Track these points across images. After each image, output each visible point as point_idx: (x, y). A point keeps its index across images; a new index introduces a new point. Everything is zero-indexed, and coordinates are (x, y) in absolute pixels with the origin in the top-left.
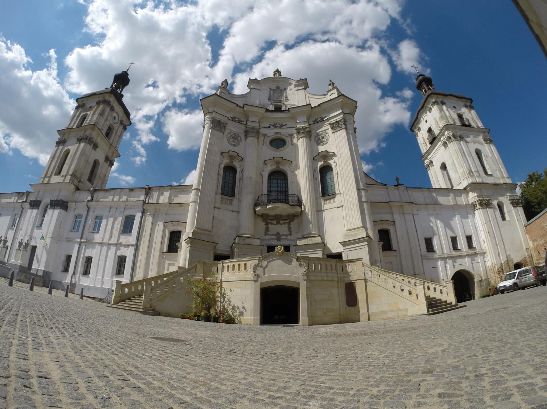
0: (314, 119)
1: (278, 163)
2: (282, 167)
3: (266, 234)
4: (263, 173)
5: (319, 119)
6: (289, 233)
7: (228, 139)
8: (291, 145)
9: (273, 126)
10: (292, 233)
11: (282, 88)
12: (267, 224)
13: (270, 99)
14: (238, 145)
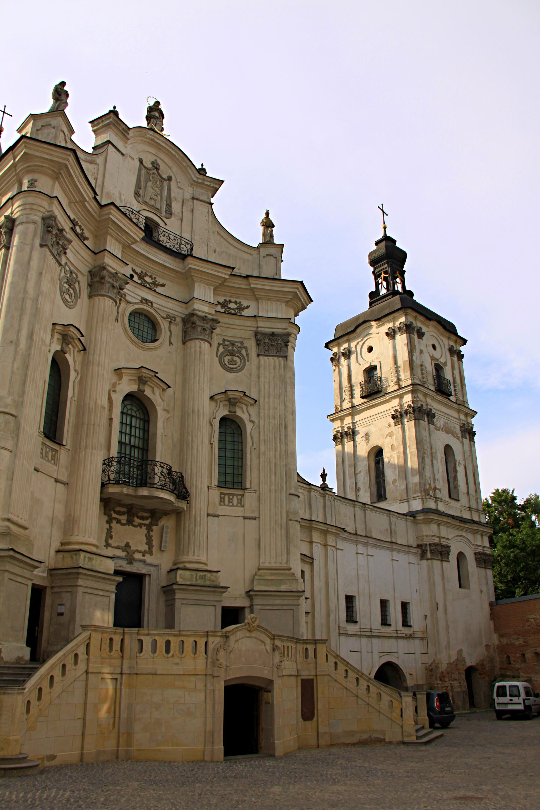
0: (221, 300)
1: (142, 380)
2: (148, 392)
3: (107, 545)
4: (113, 396)
5: (232, 306)
6: (146, 547)
8: (168, 343)
9: (141, 276)
10: (154, 550)
11: (165, 172)
12: (109, 522)
13: (137, 194)
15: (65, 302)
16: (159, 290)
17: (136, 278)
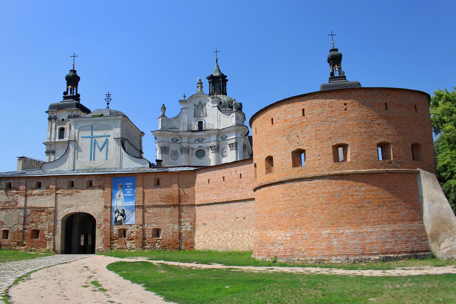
7: (171, 156)
9: (198, 140)
14: (177, 158)
15: (175, 160)
16: (204, 141)
17: (197, 142)
